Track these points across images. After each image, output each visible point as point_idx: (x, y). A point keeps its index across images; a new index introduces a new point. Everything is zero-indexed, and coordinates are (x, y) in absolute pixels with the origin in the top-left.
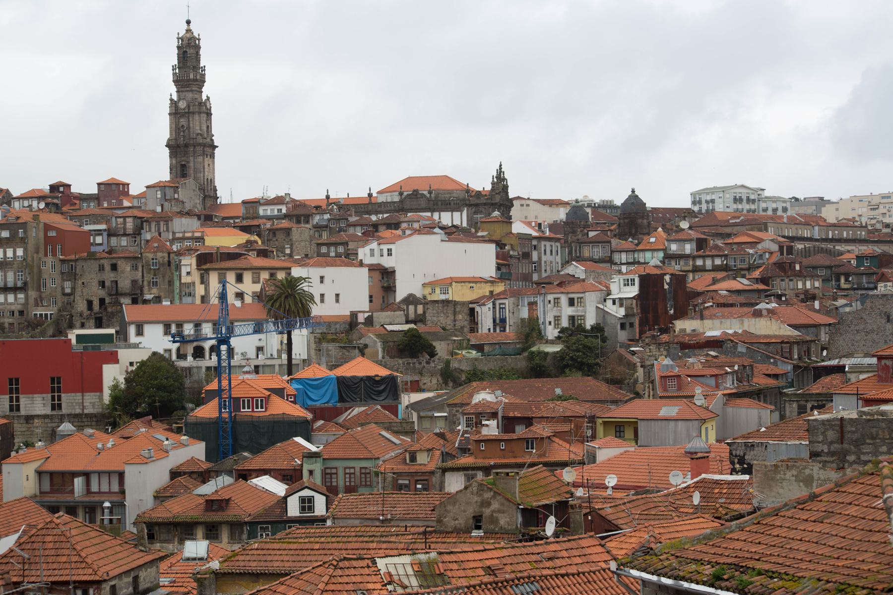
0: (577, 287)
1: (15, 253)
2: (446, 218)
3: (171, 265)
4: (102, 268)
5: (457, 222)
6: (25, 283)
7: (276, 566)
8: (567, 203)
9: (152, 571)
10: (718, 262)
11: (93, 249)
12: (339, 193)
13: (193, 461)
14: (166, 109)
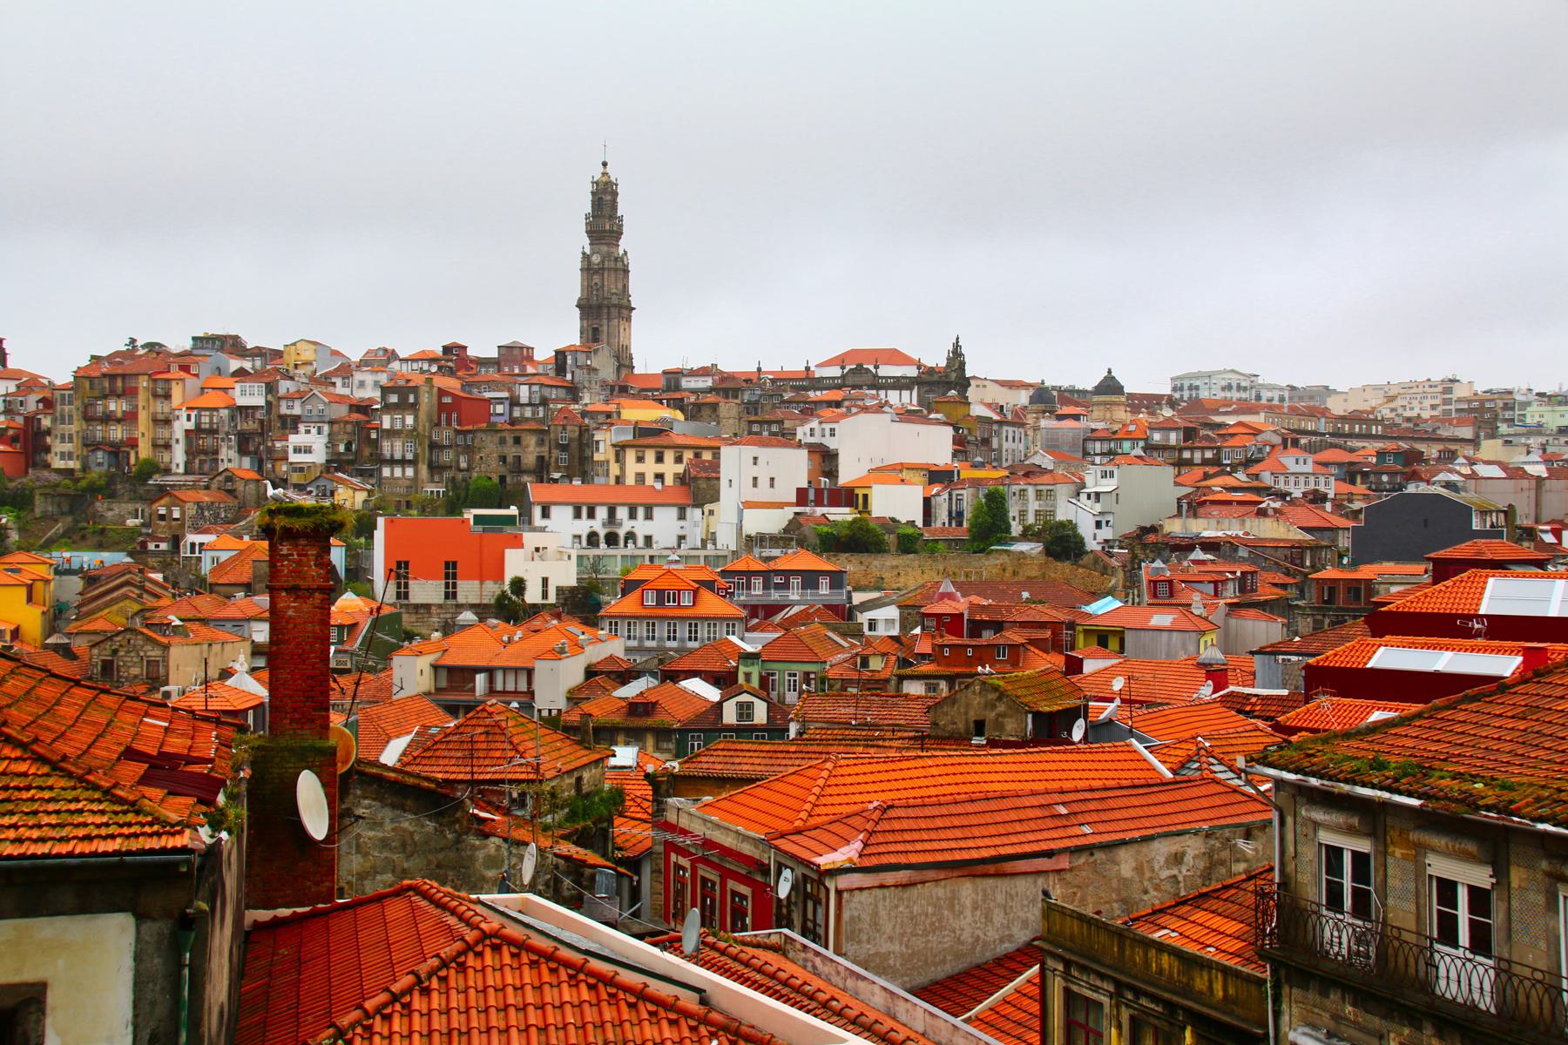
0: (1046, 478)
1: (403, 420)
2: (893, 396)
4: (503, 441)
6: (416, 455)
7: (746, 769)
8: (1030, 385)
10: (1209, 455)
11: (493, 419)
12: (771, 366)
13: (611, 659)
14: (577, 264)
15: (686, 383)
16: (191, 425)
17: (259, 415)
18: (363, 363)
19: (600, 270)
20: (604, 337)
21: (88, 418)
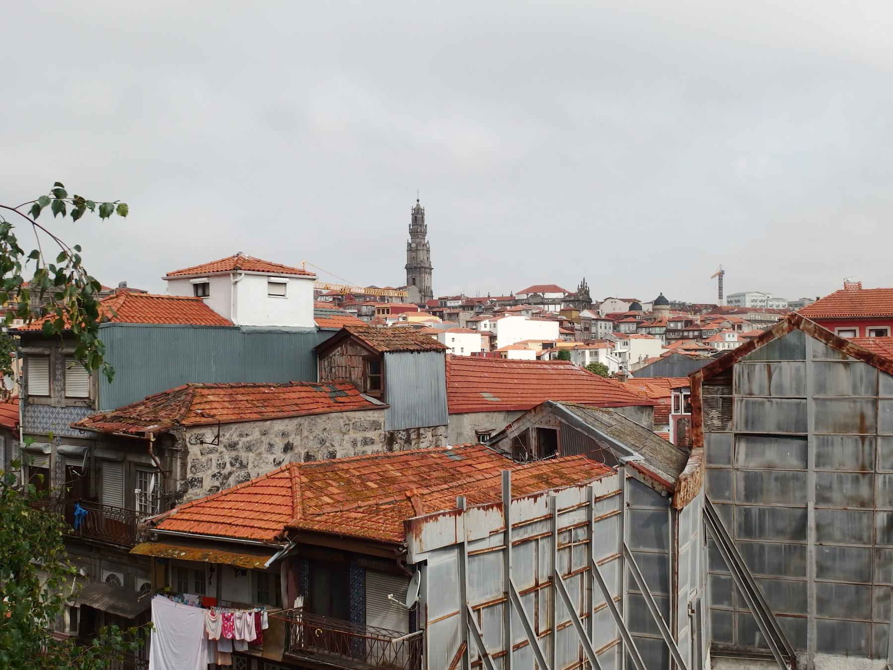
2: (552, 308)
10: (696, 333)
15: (449, 304)
20: (417, 282)
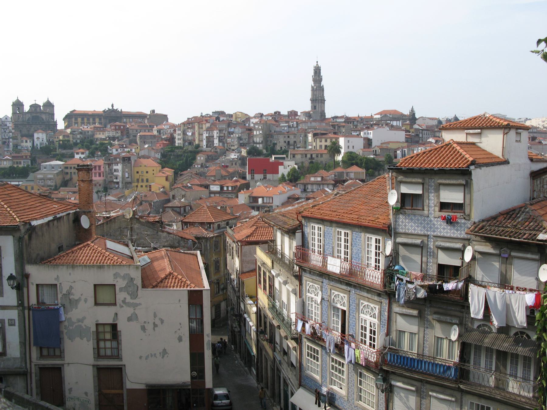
2: (395, 123)
3: (306, 136)
4: (285, 137)
5: (398, 124)
6: (262, 142)
9: (234, 221)
12: (362, 115)
13: (294, 195)
14: (310, 89)
16: (208, 135)
17: (224, 132)
18: (255, 117)
19: (316, 90)
20: (317, 108)
21: (184, 133)
